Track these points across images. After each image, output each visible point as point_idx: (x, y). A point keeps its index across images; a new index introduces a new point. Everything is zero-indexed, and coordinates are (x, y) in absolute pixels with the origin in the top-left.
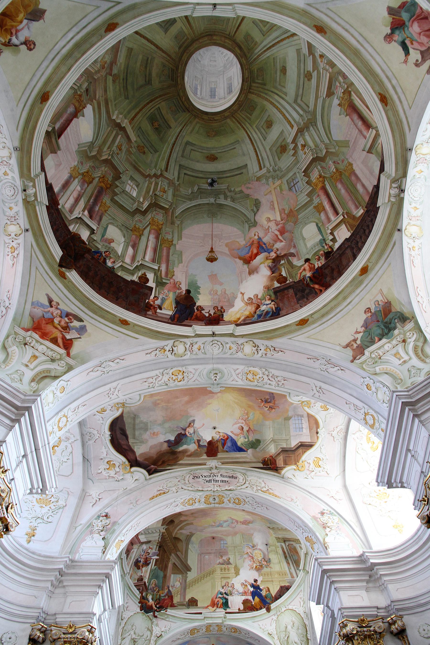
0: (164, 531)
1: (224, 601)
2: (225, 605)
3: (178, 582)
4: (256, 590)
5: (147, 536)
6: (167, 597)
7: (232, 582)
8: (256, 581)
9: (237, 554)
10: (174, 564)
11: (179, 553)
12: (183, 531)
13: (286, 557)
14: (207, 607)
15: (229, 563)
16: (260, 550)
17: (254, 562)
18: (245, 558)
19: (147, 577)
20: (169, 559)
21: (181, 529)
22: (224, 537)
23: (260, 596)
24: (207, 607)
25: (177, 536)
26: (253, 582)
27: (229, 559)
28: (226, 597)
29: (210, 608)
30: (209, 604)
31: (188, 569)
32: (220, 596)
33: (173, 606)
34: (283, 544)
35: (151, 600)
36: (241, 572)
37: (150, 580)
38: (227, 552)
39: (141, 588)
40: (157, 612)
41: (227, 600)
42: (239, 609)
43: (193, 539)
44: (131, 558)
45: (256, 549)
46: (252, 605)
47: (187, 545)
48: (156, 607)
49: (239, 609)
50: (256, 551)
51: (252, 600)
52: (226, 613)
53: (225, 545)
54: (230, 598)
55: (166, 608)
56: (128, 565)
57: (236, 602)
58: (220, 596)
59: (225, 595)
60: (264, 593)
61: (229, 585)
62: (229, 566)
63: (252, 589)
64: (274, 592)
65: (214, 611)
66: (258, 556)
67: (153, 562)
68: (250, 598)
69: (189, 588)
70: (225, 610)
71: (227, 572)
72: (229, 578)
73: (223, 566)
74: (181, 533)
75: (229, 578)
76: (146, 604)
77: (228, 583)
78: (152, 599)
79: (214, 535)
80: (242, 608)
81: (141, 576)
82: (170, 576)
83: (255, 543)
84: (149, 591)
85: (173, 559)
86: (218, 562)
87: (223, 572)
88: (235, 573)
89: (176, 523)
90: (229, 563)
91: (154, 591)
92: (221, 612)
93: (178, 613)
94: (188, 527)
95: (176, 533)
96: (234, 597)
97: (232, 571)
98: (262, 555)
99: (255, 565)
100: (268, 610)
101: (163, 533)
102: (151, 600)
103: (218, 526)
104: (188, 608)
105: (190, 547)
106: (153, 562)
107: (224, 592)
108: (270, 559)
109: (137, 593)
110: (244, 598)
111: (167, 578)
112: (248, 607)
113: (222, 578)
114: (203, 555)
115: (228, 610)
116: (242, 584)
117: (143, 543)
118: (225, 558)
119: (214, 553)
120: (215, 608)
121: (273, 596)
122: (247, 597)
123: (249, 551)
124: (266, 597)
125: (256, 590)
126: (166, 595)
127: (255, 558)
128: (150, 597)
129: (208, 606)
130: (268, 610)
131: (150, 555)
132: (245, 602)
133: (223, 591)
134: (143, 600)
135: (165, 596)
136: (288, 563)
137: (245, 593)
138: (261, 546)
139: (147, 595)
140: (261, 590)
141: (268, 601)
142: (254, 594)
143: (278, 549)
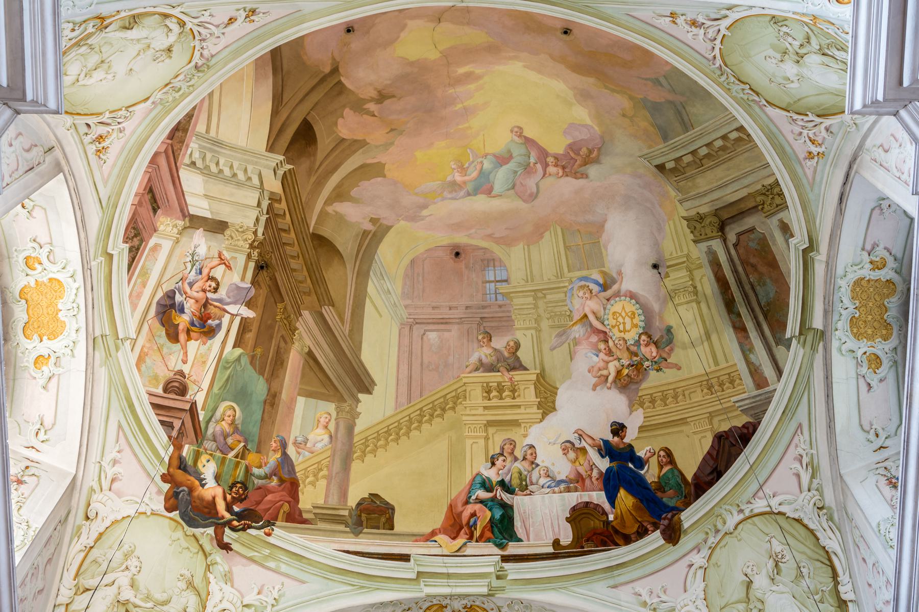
0: (275, 185)
1: (498, 514)
2: (503, 528)
3: (320, 431)
4: (621, 465)
5: (217, 189)
6: (275, 482)
7: (528, 441)
8: (618, 429)
9: (545, 324)
10: (310, 354)
11: (329, 313)
12: (344, 208)
13: (730, 305)
14: (430, 537)
15: (516, 365)
16: (632, 296)
17: (610, 353)
18: (577, 342)
19: (205, 385)
20: (293, 330)
21: (340, 195)
22: (498, 251)
23: (637, 486)
24: (430, 537)
25: (326, 232)
26: (609, 437)
27: (518, 346)
28: (506, 497)
29: (442, 538)
30: (438, 524)
31: (363, 383)
32: (482, 494)
33: (295, 517)
34: (717, 245)
35: (211, 482)
36: (562, 398)
37: (214, 400)
38: (509, 319)
39: (177, 424)
40: (234, 529)
41: (507, 509)
42: (556, 543)
43: (385, 252)
44: (145, 274)
45: (617, 294)
46: (608, 523)
47: (363, 276)
48: (229, 509)
49: (556, 543)
50: (617, 306)
51: (607, 506)
52: (506, 559)
53: (503, 288)
54: (520, 502)
55: (270, 523)
56: (134, 306)
57: (544, 515)
58: (482, 494)
59: (500, 494)
60: (651, 473)
61: (518, 453)
62: (518, 376)
63: (604, 464)
64: (689, 466)
65: (458, 553)
66: (624, 322)
67: (229, 327)
68: (598, 497)
69: (362, 458)
70: (502, 546)
71: (508, 401)
72: (515, 423)
73: (494, 378)
74: (340, 219)
75: (515, 423)
76: (191, 490)
77: (513, 443)
78: (217, 478)
79: (461, 239)
80: (567, 537)
81: (181, 373)
82: (293, 401)
83: (611, 267)
84: (209, 445)
85: (306, 334)
86: (474, 359)
87: (495, 402)
88: (540, 405)
89: (321, 153)
90: (516, 365)
91: (225, 449)
92: (483, 558)
93: (314, 545)
94: (367, 188)
95: (323, 214)
96: (537, 498)
97: (529, 395)
98: (639, 320)
99: (613, 367)
100: (673, 535)
101: (274, 198)
102: (211, 482)
103: (476, 191)
104: (357, 534)
105: (371, 289)
106: (229, 327)
107: (495, 479)
108: (669, 330)
109: (160, 438)
110: (574, 498)
111: (282, 408)
112: (592, 533)
113: (490, 424)
114: (418, 330)
115: (513, 549)
116: (568, 446)
117: (195, 222)
118: (500, 343)
119: (461, 321)
120: (460, 541)
121: (689, 477)
122: (585, 497)
123: (592, 305)
124: (661, 485)
125: (621, 465)
126: (274, 473)
127: (616, 334)
128: (208, 469)
129: (434, 533)
130: (673, 535)
131: (222, 293)
132: (580, 515)
133: (492, 475)
134: (179, 475)
135: (267, 477)
136: (740, 329)
137: (578, 482)
138: (635, 279)
139: (197, 455)
140: (640, 463)
141: (669, 499)
142: (610, 484)
143: (697, 274)
